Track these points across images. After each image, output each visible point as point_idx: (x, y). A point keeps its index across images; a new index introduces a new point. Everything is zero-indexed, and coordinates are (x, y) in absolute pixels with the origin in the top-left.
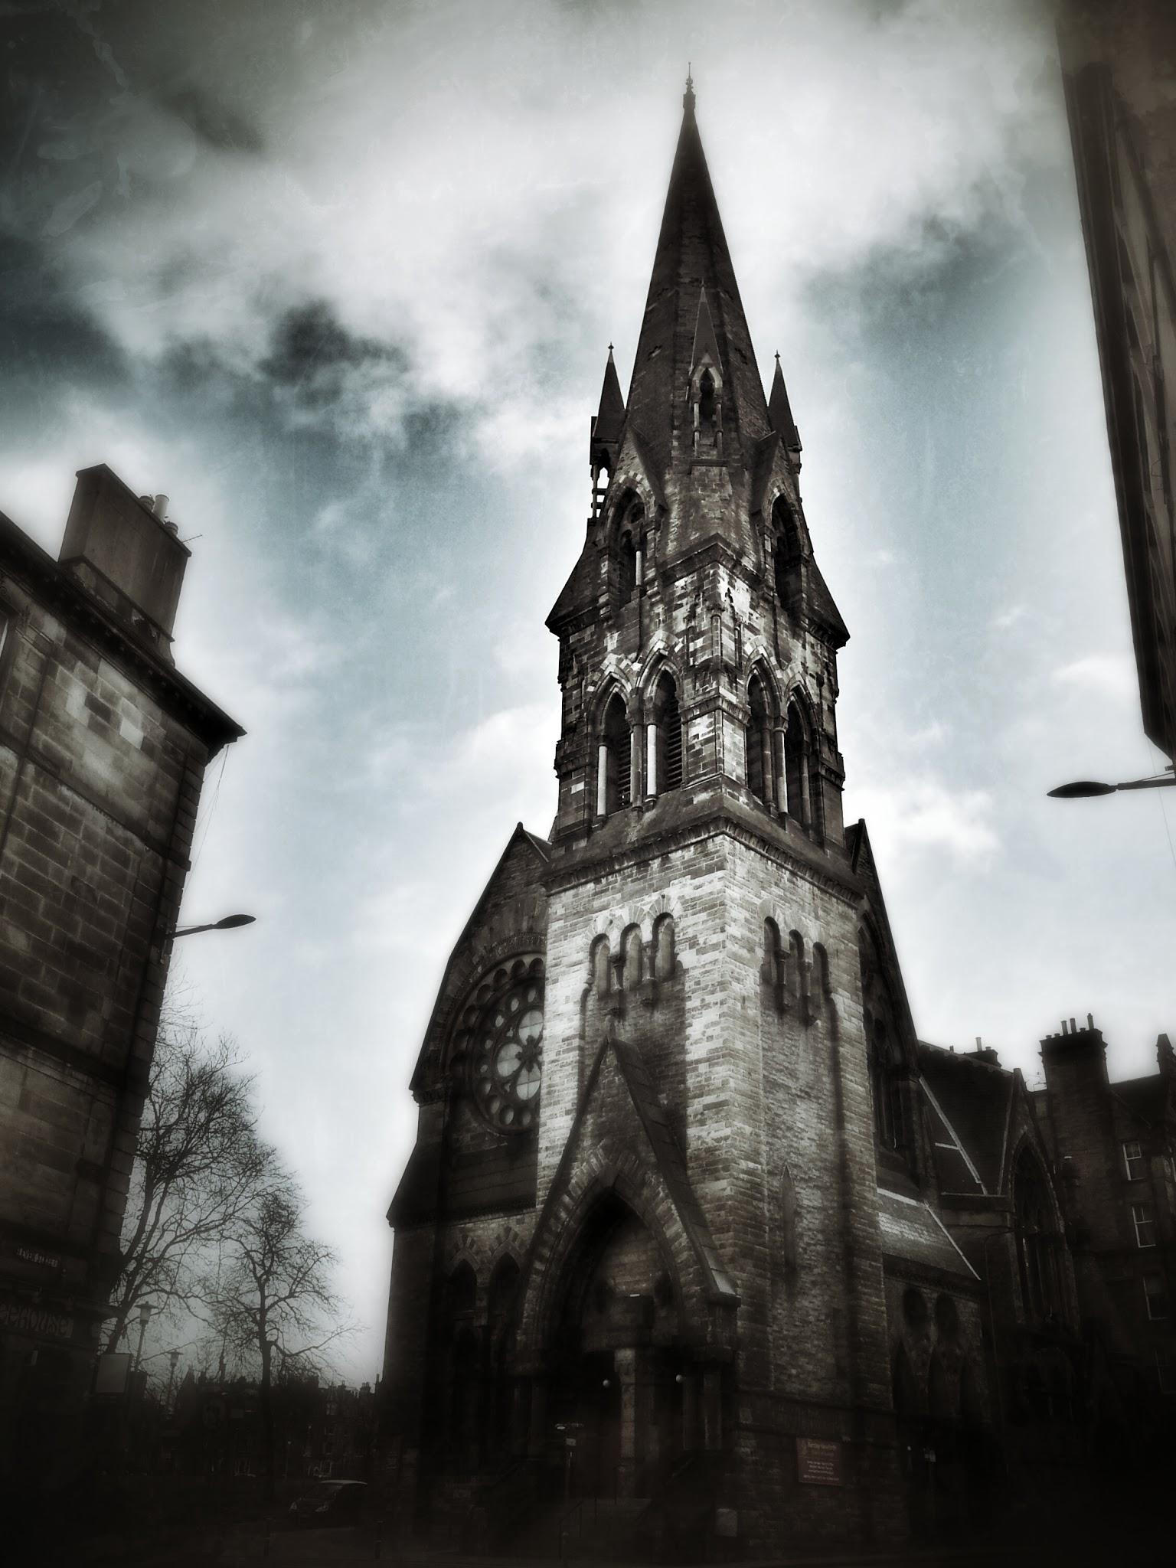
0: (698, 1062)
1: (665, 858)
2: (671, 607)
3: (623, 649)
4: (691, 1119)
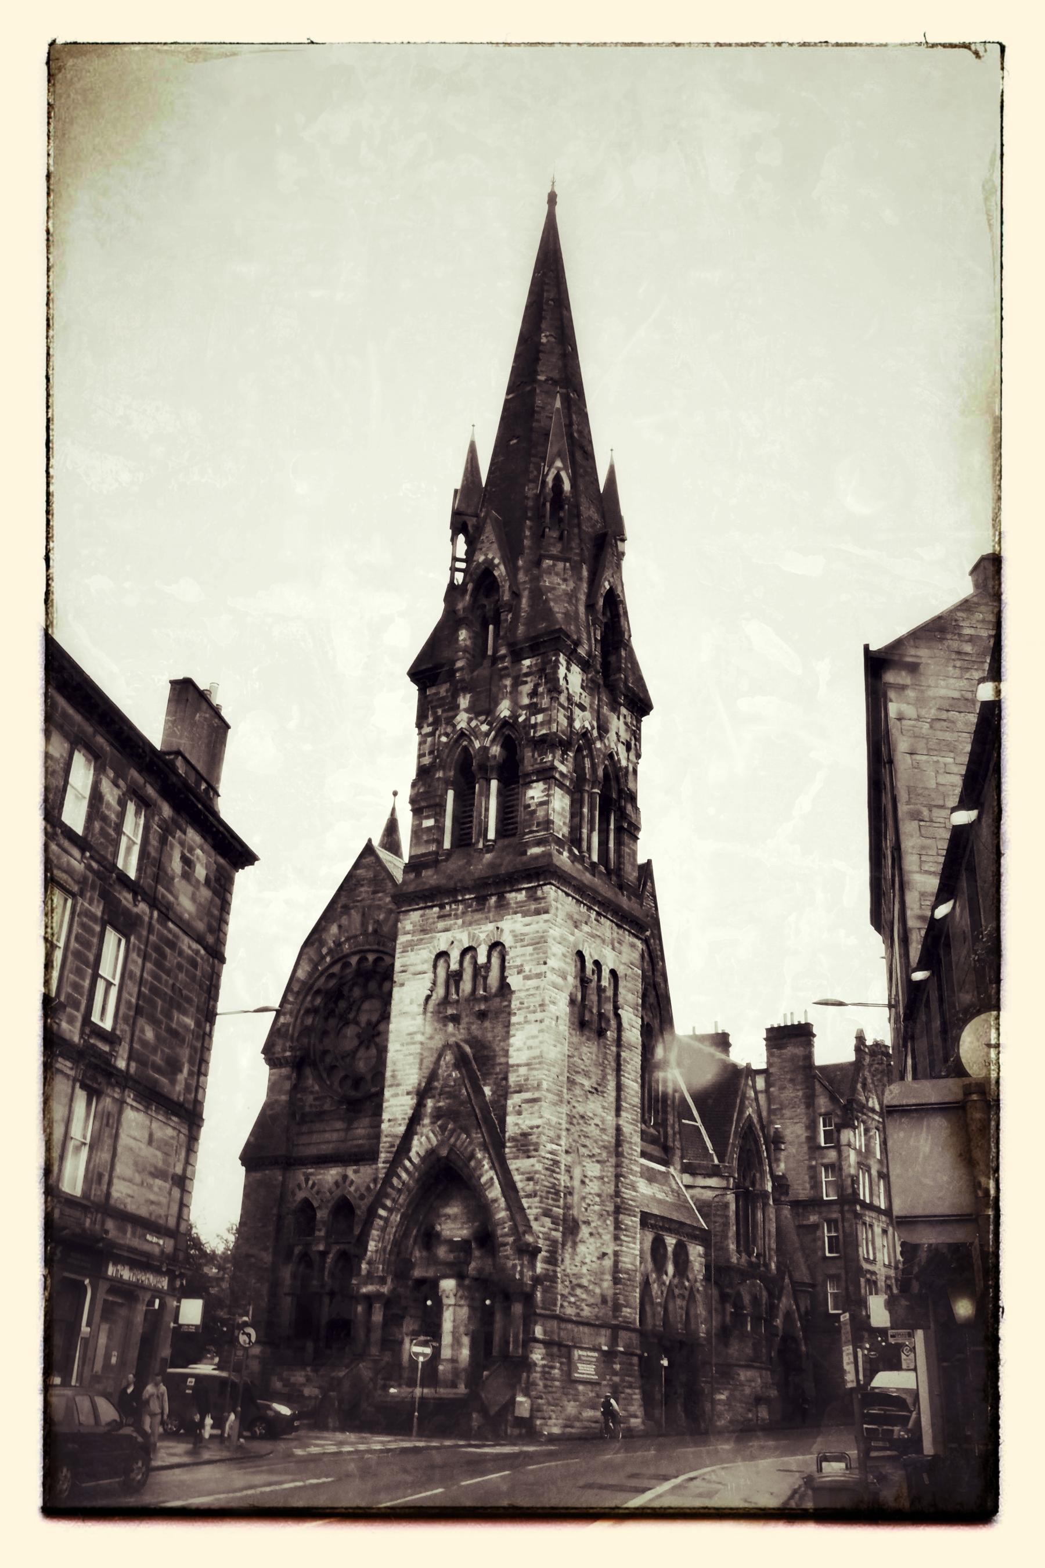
0: (518, 1065)
1: (501, 897)
2: (518, 682)
3: (474, 710)
4: (510, 1109)
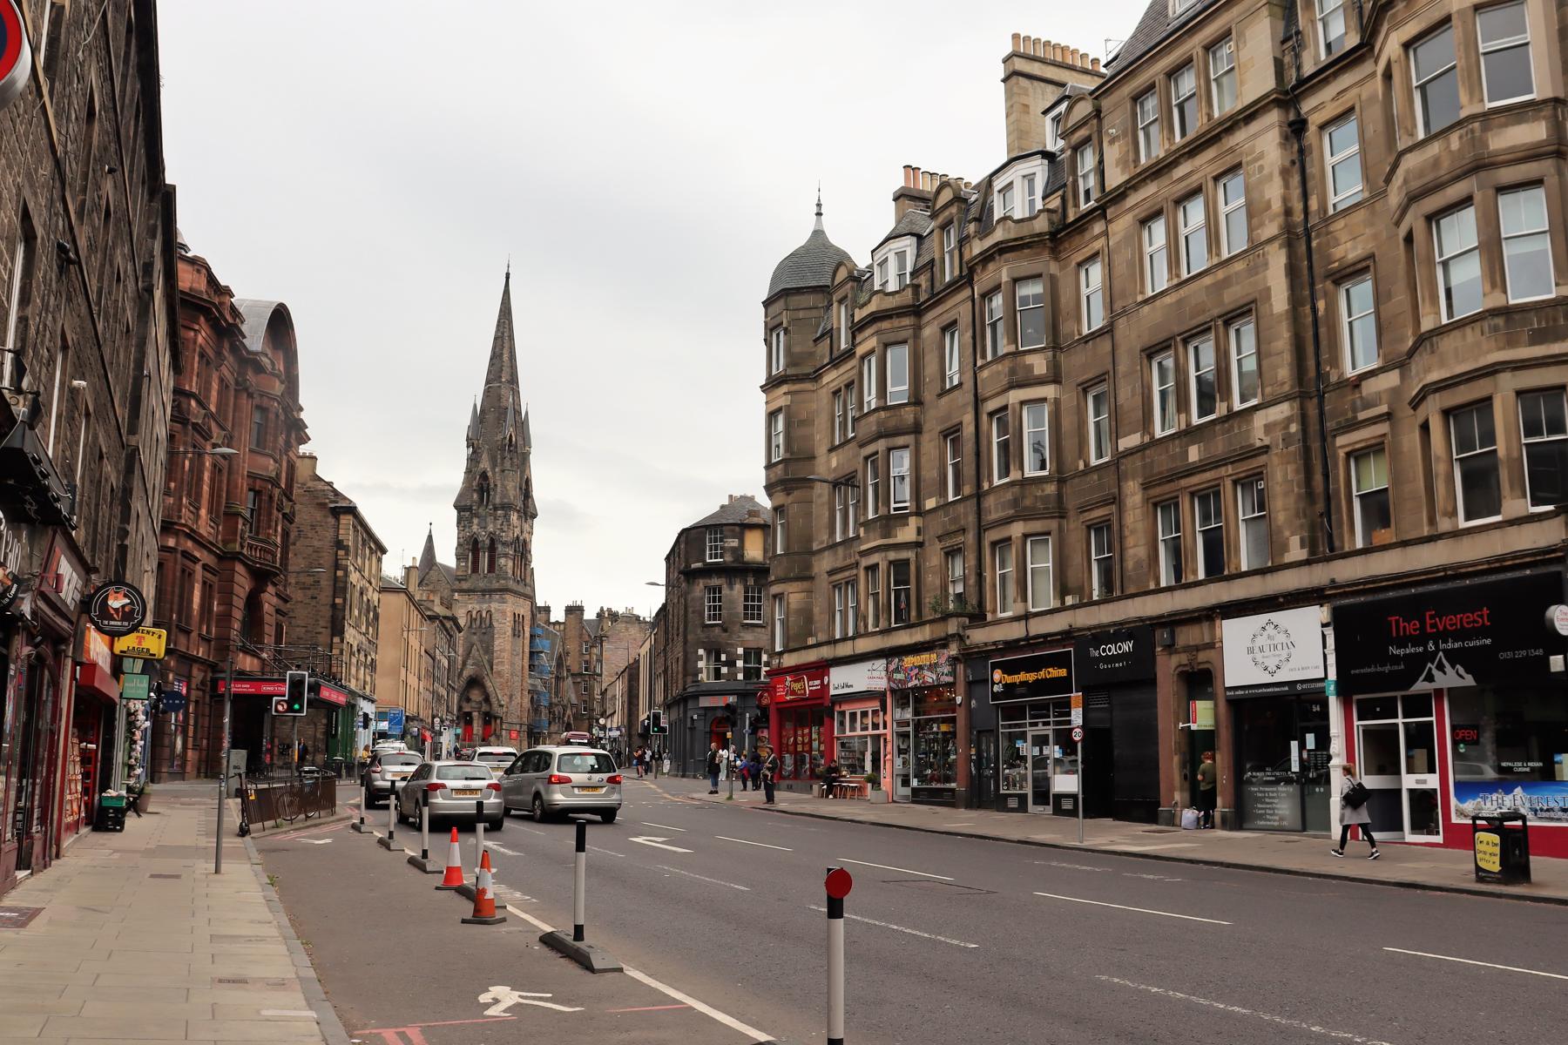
1: (490, 595)
2: (496, 519)
